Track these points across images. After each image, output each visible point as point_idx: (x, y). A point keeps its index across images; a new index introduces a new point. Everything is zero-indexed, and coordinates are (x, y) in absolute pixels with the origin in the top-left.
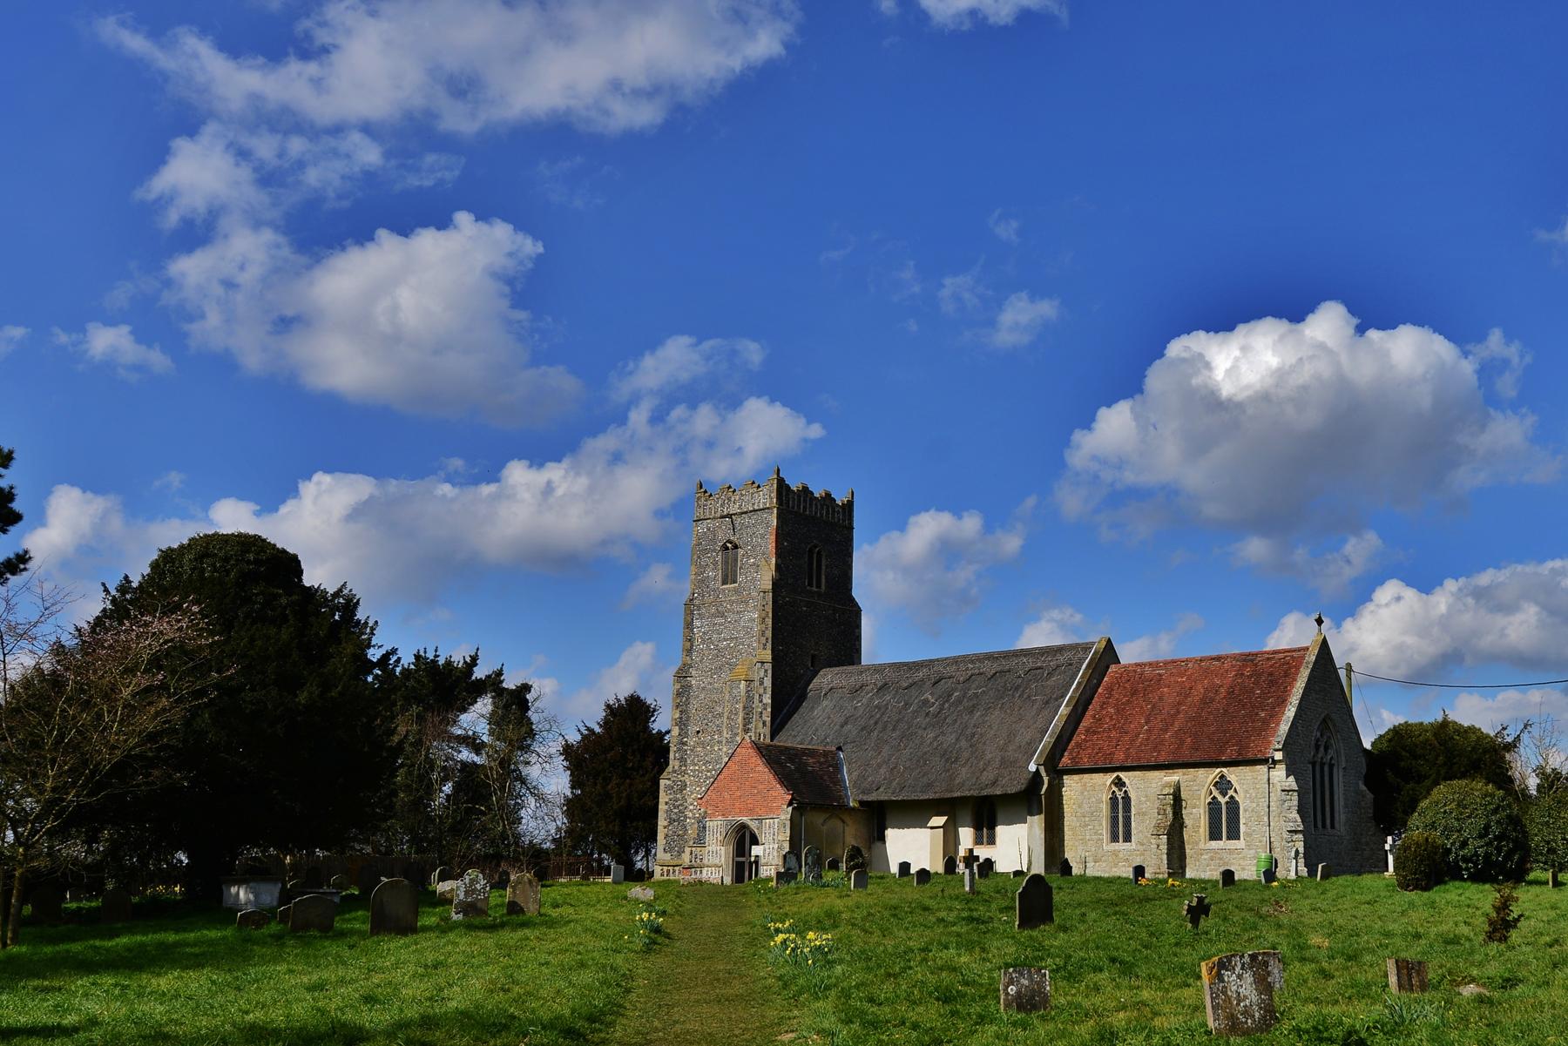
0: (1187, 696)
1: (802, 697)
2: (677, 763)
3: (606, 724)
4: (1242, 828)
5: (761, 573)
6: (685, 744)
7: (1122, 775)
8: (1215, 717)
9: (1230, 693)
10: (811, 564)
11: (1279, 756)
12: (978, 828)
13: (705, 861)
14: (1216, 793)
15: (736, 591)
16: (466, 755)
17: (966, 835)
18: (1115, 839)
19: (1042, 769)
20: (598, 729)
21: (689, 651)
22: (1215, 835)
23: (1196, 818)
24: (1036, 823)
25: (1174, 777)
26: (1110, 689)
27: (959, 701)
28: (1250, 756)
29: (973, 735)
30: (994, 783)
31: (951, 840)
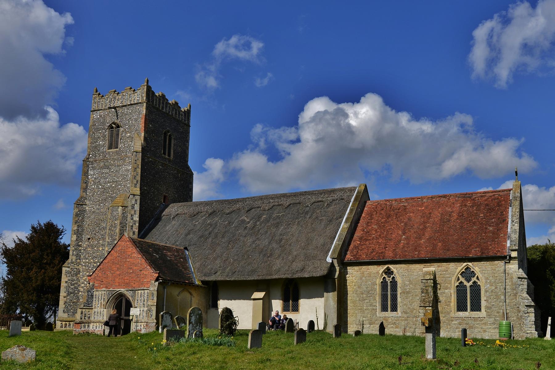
0: (429, 218)
1: (158, 219)
2: (74, 258)
3: (31, 238)
4: (483, 303)
5: (134, 140)
6: (80, 246)
7: (391, 266)
9: (460, 215)
10: (165, 141)
11: (514, 254)
12: (286, 300)
13: (92, 319)
14: (462, 279)
15: (117, 153)
17: (277, 305)
18: (384, 308)
19: (335, 262)
20: (26, 240)
21: (85, 189)
22: (461, 307)
23: (448, 296)
24: (331, 297)
25: (432, 268)
26: (370, 214)
27: (267, 220)
28: (491, 254)
29: (281, 240)
30: (302, 270)
31: (267, 308)
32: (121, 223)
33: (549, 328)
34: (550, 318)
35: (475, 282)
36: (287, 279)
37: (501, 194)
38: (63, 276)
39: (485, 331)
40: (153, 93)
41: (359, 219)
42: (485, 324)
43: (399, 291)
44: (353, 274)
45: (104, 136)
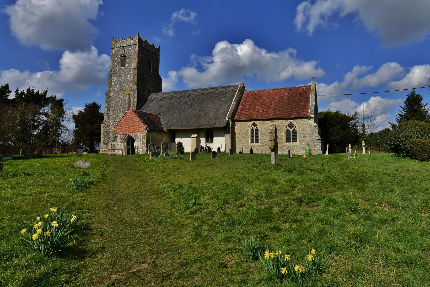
1: (146, 101)
2: (107, 119)
3: (85, 110)
6: (109, 114)
7: (256, 122)
8: (293, 103)
9: (288, 98)
11: (312, 116)
12: (207, 138)
13: (116, 148)
14: (288, 128)
15: (125, 69)
16: (44, 118)
17: (203, 141)
18: (253, 141)
19: (230, 120)
20: (83, 111)
21: (110, 87)
22: (288, 140)
23: (282, 135)
24: (228, 137)
25: (274, 123)
26: (246, 98)
27: (197, 101)
28: (302, 116)
29: (204, 110)
30: (214, 124)
32: (128, 103)
33: (327, 150)
34: (328, 145)
35: (294, 129)
36: (207, 128)
37: (307, 88)
38: (102, 128)
39: (299, 151)
40: (141, 40)
41: (240, 100)
42: (299, 148)
43: (259, 133)
44: (238, 126)
45: (118, 61)
